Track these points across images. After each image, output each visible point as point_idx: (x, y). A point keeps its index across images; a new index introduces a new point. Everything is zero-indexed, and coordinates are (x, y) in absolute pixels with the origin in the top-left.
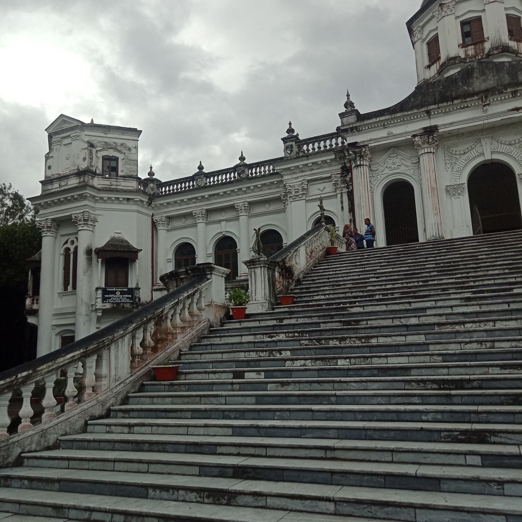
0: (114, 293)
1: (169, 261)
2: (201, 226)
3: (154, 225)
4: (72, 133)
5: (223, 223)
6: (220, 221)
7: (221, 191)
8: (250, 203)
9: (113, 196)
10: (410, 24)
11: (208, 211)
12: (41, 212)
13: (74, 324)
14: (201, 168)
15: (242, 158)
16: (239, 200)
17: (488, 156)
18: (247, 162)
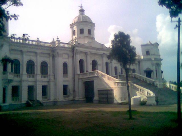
5: (31, 57)
6: (30, 55)
11: (28, 52)
15: (38, 39)
17: (96, 59)
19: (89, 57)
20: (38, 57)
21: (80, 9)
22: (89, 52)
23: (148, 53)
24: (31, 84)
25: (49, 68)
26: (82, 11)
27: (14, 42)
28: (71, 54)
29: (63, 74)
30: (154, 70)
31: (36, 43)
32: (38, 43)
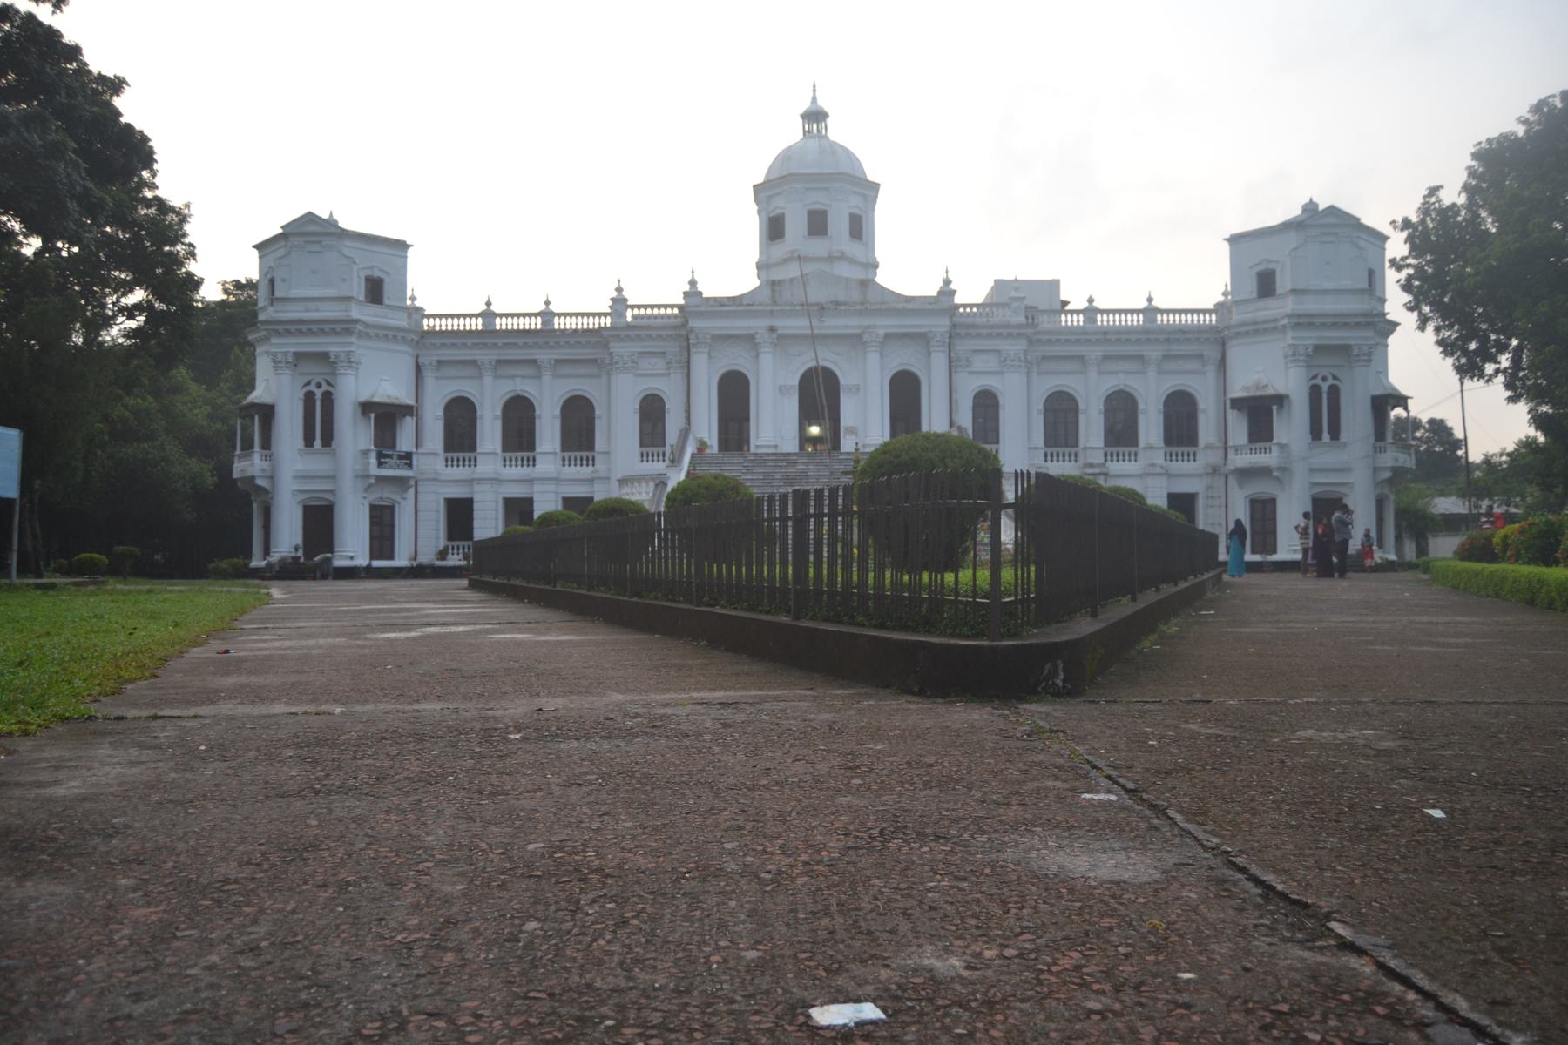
0: (390, 456)
1: (437, 418)
2: (488, 379)
3: (418, 369)
4: (327, 241)
5: (518, 380)
7: (520, 341)
8: (557, 361)
9: (382, 332)
10: (755, 187)
12: (274, 340)
13: (332, 492)
14: (488, 304)
15: (547, 303)
16: (544, 356)
18: (554, 308)
19: (766, 359)
20: (547, 378)
21: (805, 105)
22: (772, 329)
23: (1266, 284)
24: (517, 491)
25: (597, 422)
26: (815, 116)
27: (432, 333)
28: (673, 348)
29: (642, 445)
30: (1293, 397)
31: (536, 324)
32: (543, 323)
